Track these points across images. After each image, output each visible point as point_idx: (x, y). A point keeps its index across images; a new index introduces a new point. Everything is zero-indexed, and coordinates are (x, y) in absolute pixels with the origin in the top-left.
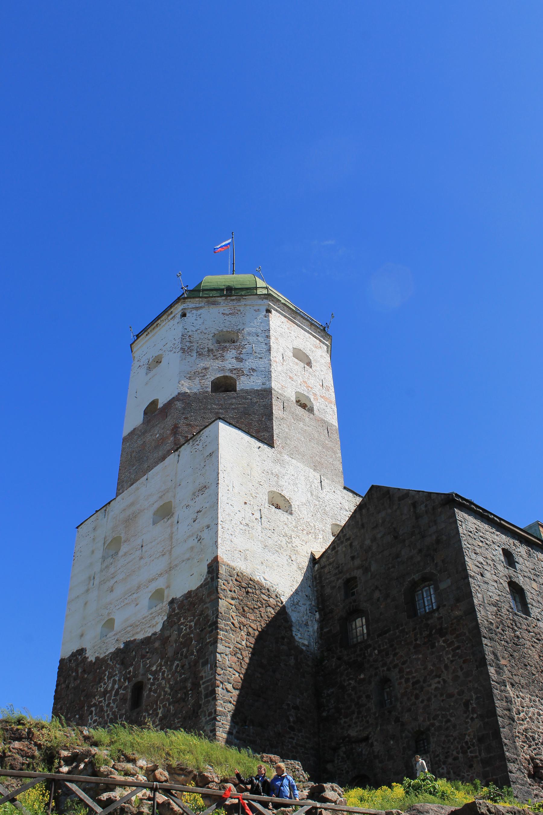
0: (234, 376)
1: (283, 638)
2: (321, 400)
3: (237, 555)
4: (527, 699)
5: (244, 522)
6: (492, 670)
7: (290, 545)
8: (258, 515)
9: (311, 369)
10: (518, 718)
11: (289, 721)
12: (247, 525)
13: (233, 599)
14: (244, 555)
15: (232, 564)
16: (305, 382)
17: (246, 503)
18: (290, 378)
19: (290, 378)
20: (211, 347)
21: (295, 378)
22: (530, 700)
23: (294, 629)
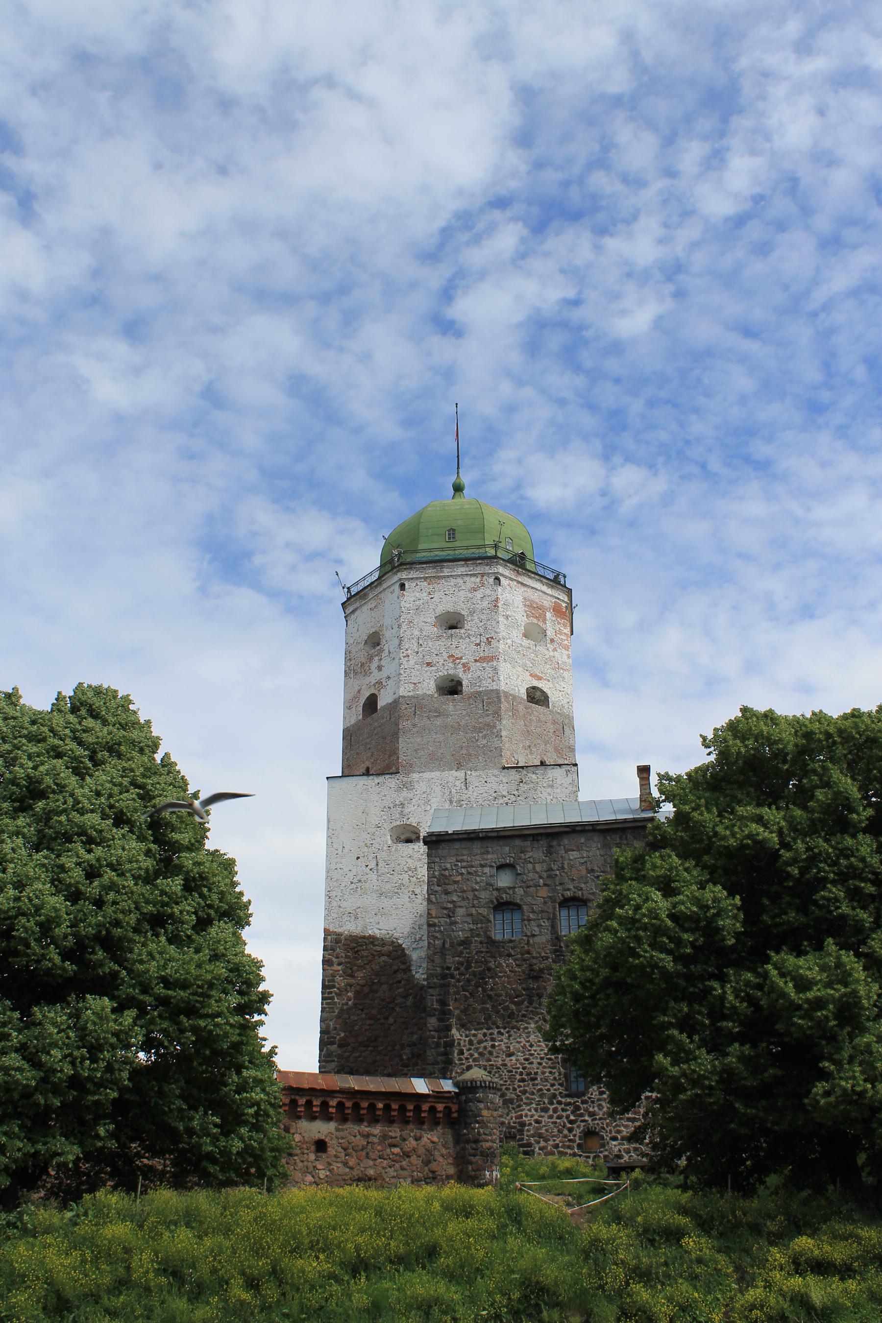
0: (376, 692)
1: (399, 982)
2: (474, 666)
3: (346, 918)
4: (480, 1036)
5: (355, 880)
6: (433, 1022)
7: (414, 879)
8: (372, 865)
9: (462, 631)
10: (460, 1059)
11: (402, 1060)
12: (360, 881)
13: (339, 964)
14: (355, 915)
15: (339, 930)
16: (452, 656)
17: (358, 858)
18: (429, 664)
19: (429, 664)
20: (363, 660)
21: (435, 659)
22: (485, 1035)
23: (413, 968)
